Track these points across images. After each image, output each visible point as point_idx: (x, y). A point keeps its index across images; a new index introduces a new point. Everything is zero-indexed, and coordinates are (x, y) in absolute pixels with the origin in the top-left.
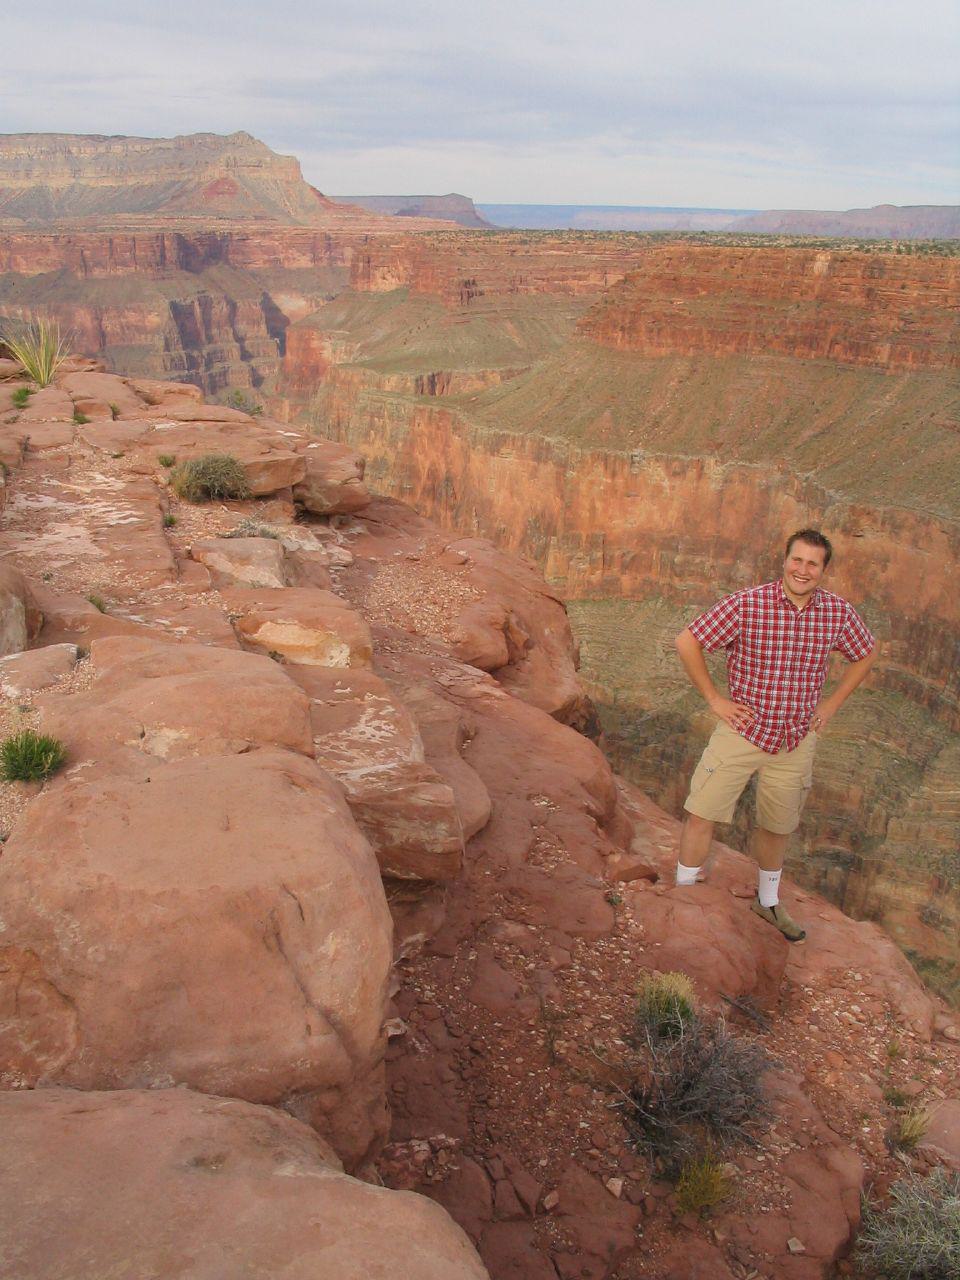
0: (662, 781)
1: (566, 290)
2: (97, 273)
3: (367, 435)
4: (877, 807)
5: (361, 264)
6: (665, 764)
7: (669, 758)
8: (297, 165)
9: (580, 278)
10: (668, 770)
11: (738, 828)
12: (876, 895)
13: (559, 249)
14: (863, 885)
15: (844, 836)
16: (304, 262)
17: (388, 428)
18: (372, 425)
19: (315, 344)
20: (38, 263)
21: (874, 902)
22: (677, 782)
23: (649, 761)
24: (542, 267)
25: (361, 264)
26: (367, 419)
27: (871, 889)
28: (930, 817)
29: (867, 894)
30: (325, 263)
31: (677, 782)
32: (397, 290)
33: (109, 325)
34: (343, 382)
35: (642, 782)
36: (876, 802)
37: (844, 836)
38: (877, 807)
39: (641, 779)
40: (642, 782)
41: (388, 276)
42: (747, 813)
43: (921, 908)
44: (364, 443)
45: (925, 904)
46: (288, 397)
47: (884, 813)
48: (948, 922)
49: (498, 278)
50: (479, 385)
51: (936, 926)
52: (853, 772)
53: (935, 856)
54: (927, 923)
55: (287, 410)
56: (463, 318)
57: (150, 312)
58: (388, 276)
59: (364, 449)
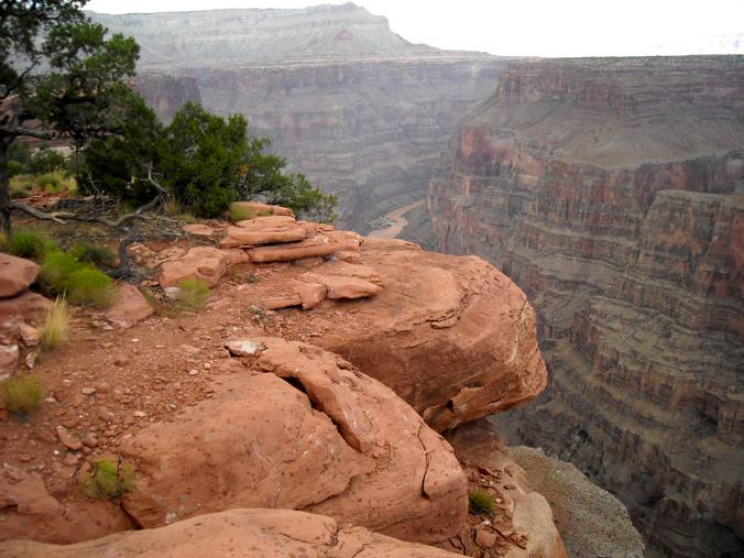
1: (690, 101)
2: (294, 90)
3: (667, 226)
5: (513, 83)
8: (386, 21)
9: (698, 91)
13: (681, 70)
16: (412, 80)
17: (692, 222)
18: (672, 218)
19: (486, 138)
20: (253, 86)
24: (675, 82)
25: (513, 83)
26: (666, 214)
30: (425, 80)
32: (540, 100)
33: (303, 124)
34: (570, 173)
41: (535, 90)
44: (664, 232)
46: (467, 175)
49: (648, 93)
50: (667, 173)
55: (468, 184)
56: (634, 123)
57: (330, 116)
58: (535, 90)
59: (663, 237)
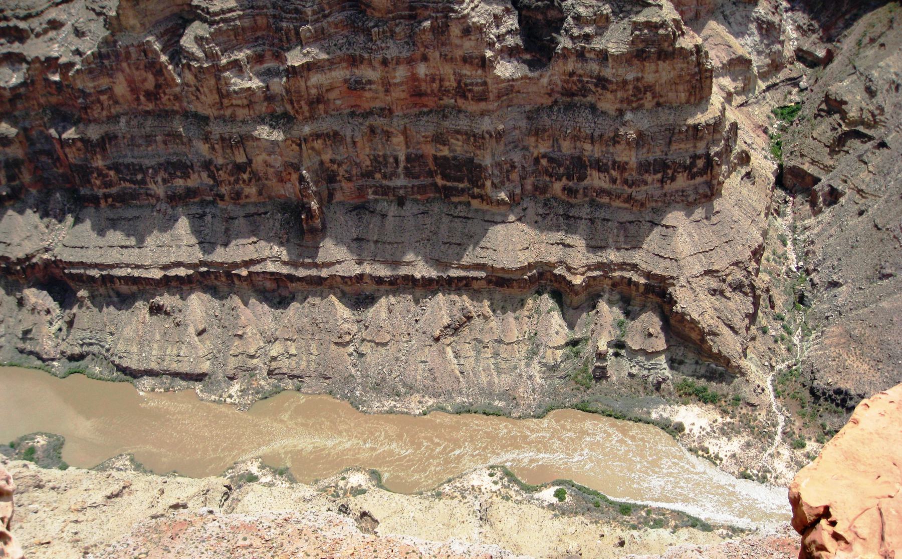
0: (111, 76)
4: (284, 25)
6: (106, 62)
7: (108, 56)
10: (112, 66)
11: (188, 85)
12: (313, 86)
14: (303, 84)
15: (268, 55)
21: (313, 91)
22: (123, 71)
23: (93, 66)
27: (309, 84)
28: (325, 16)
29: (307, 87)
31: (123, 71)
35: (96, 83)
36: (281, 21)
37: (268, 55)
38: (284, 25)
39: (94, 81)
40: (96, 83)
42: (190, 69)
43: (346, 81)
45: (348, 77)
47: (291, 26)
48: (370, 82)
51: (363, 89)
52: (252, 7)
53: (341, 41)
54: (355, 89)
